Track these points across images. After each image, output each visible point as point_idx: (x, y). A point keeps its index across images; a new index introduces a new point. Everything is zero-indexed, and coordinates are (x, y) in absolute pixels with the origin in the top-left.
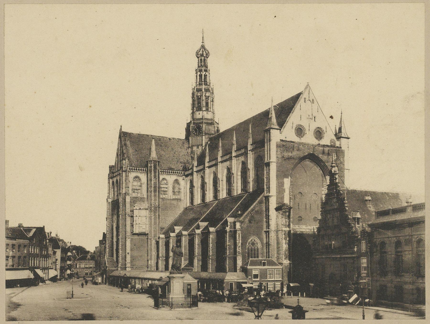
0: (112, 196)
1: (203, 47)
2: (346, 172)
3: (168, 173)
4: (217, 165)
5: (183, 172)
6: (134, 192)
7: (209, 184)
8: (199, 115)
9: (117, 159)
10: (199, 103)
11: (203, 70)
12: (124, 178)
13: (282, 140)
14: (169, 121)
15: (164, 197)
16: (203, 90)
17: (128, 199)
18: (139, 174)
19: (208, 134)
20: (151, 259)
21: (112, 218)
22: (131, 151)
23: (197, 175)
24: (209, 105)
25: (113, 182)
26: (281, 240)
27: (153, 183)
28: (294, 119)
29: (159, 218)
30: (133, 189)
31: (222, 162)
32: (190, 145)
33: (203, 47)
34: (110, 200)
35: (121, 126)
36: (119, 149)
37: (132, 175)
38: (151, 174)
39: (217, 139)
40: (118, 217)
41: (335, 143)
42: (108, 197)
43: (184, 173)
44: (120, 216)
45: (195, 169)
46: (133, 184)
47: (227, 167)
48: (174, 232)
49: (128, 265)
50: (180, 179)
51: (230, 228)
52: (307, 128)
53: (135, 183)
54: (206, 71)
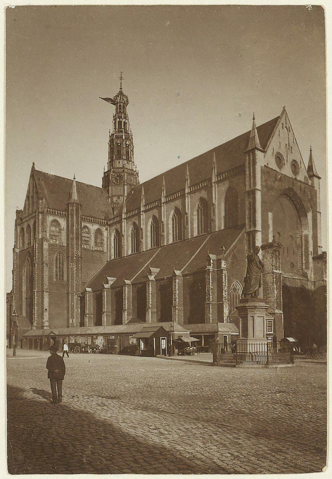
0: (20, 244)
1: (121, 93)
2: (318, 214)
3: (90, 222)
4: (161, 207)
5: (106, 221)
6: (52, 238)
7: (146, 231)
8: (119, 164)
9: (27, 203)
10: (119, 152)
11: (123, 117)
12: (40, 221)
13: (265, 166)
14: (88, 167)
15: (85, 247)
16: (124, 138)
17: (46, 246)
18: (58, 219)
19: (130, 185)
20: (73, 317)
21: (20, 271)
22: (46, 192)
23: (127, 223)
24: (130, 155)
25: (22, 229)
26: (270, 285)
27: (75, 229)
28: (276, 143)
29: (81, 271)
30: (50, 235)
31: (166, 203)
32: (110, 195)
33: (121, 93)
34: (17, 251)
35: (34, 163)
36: (31, 190)
37: (50, 218)
38: (72, 219)
39: (136, 191)
40: (33, 265)
41: (308, 182)
42: (15, 246)
43: (107, 223)
44: (36, 264)
45: (124, 216)
46: (50, 229)
47: (176, 207)
48: (107, 283)
49: (47, 324)
50: (103, 229)
51: (213, 267)
52: (285, 158)
53: (53, 229)
54: (125, 118)
